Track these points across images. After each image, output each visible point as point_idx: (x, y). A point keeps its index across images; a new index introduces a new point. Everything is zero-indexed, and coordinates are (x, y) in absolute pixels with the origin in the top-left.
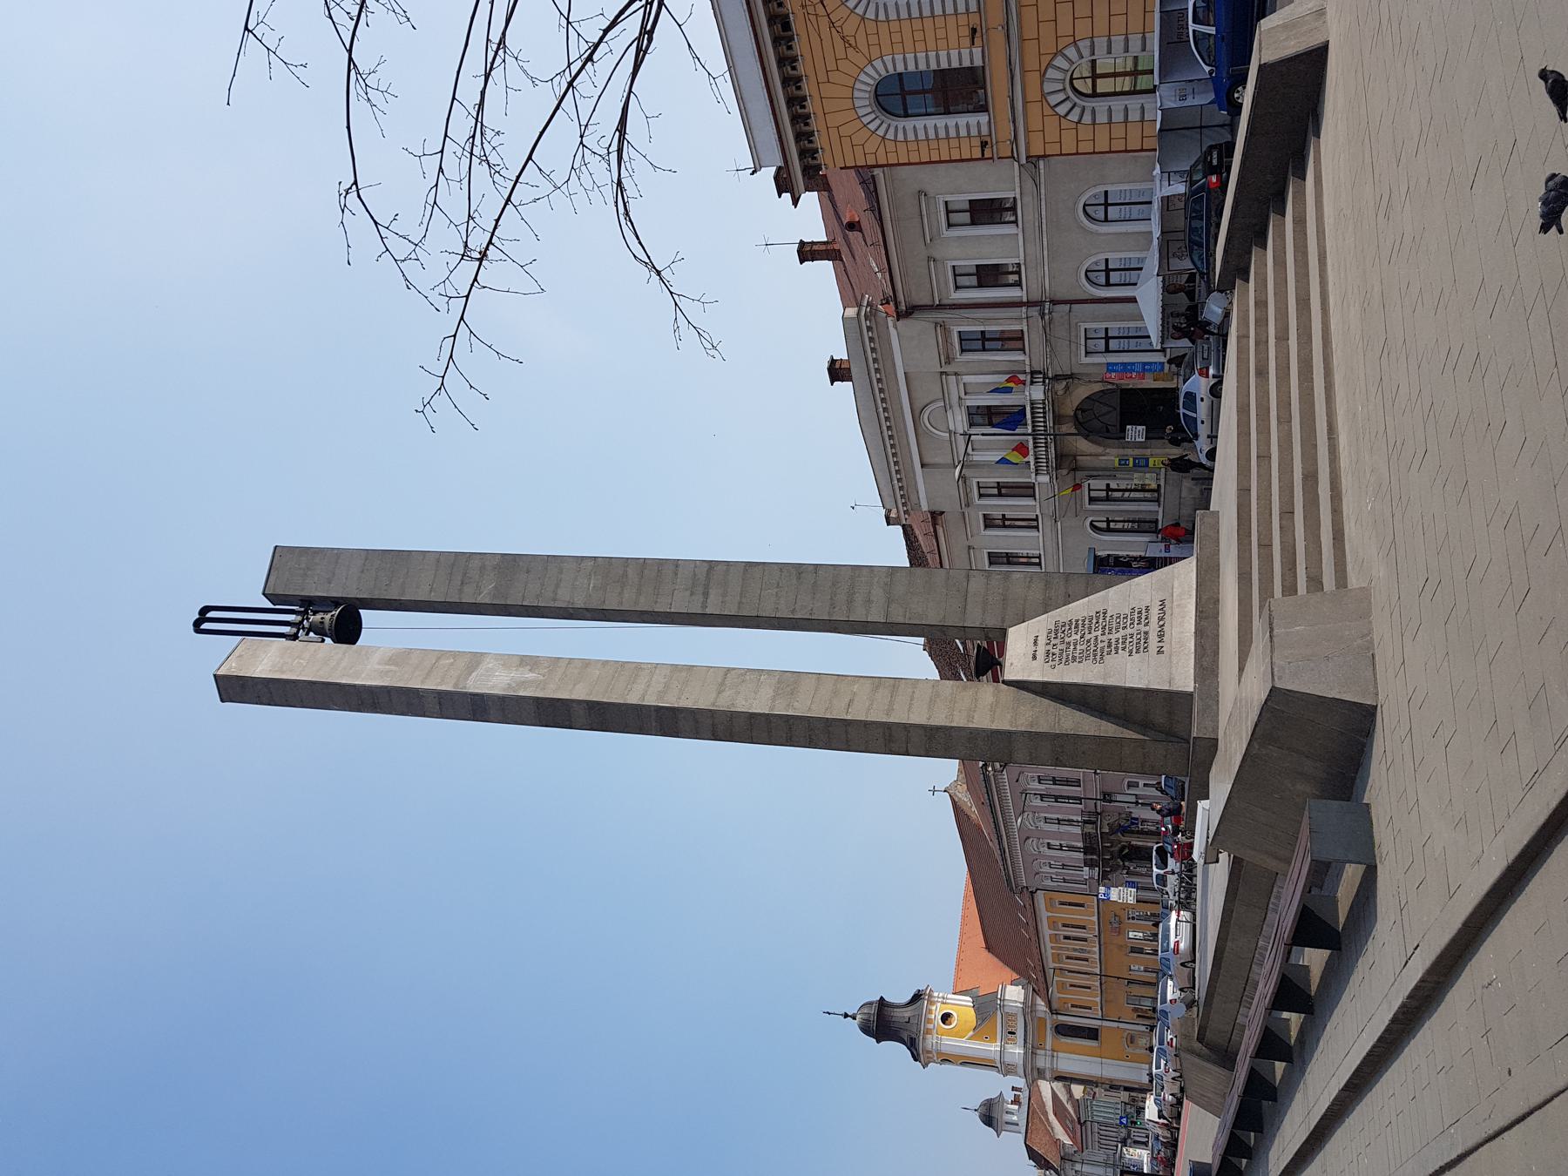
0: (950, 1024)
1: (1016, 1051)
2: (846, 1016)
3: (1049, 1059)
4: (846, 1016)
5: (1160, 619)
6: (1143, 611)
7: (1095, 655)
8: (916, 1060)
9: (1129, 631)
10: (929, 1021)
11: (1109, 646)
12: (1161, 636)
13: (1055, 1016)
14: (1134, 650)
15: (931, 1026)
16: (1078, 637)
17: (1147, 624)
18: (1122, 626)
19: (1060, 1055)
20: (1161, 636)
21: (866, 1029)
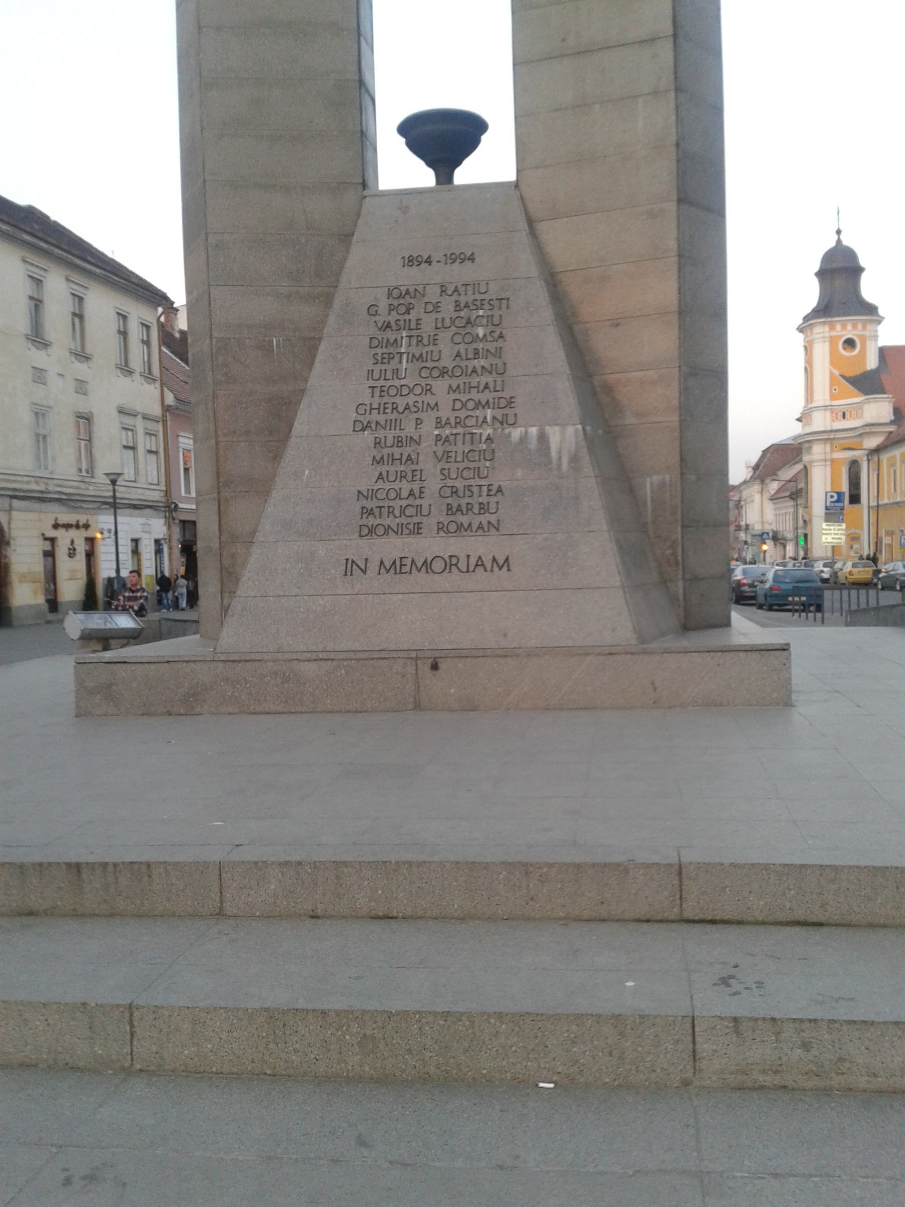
0: (844, 349)
1: (821, 422)
2: (839, 232)
3: (822, 457)
4: (839, 232)
5: (451, 564)
6: (484, 519)
7: (382, 409)
8: (804, 318)
9: (433, 484)
10: (844, 327)
11: (399, 442)
12: (397, 567)
13: (865, 458)
14: (370, 504)
15: (838, 327)
16: (447, 362)
17: (441, 527)
18: (453, 466)
19: (828, 469)
20: (397, 567)
21: (829, 256)
